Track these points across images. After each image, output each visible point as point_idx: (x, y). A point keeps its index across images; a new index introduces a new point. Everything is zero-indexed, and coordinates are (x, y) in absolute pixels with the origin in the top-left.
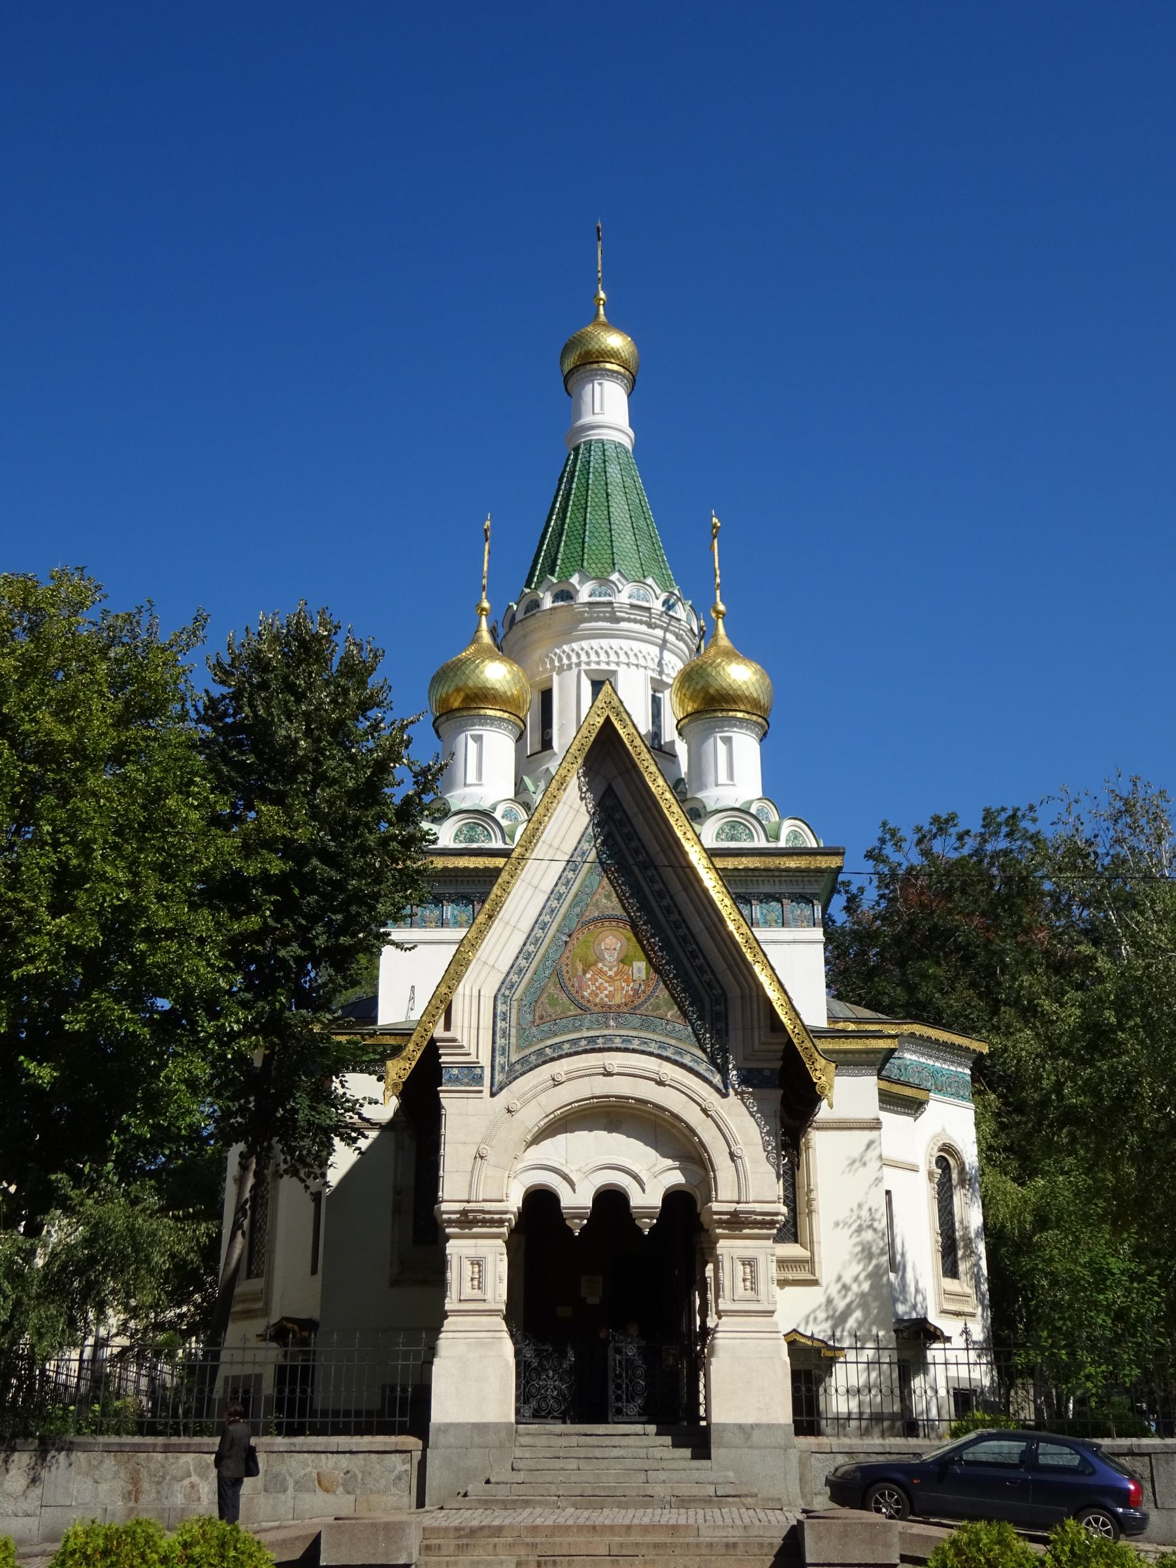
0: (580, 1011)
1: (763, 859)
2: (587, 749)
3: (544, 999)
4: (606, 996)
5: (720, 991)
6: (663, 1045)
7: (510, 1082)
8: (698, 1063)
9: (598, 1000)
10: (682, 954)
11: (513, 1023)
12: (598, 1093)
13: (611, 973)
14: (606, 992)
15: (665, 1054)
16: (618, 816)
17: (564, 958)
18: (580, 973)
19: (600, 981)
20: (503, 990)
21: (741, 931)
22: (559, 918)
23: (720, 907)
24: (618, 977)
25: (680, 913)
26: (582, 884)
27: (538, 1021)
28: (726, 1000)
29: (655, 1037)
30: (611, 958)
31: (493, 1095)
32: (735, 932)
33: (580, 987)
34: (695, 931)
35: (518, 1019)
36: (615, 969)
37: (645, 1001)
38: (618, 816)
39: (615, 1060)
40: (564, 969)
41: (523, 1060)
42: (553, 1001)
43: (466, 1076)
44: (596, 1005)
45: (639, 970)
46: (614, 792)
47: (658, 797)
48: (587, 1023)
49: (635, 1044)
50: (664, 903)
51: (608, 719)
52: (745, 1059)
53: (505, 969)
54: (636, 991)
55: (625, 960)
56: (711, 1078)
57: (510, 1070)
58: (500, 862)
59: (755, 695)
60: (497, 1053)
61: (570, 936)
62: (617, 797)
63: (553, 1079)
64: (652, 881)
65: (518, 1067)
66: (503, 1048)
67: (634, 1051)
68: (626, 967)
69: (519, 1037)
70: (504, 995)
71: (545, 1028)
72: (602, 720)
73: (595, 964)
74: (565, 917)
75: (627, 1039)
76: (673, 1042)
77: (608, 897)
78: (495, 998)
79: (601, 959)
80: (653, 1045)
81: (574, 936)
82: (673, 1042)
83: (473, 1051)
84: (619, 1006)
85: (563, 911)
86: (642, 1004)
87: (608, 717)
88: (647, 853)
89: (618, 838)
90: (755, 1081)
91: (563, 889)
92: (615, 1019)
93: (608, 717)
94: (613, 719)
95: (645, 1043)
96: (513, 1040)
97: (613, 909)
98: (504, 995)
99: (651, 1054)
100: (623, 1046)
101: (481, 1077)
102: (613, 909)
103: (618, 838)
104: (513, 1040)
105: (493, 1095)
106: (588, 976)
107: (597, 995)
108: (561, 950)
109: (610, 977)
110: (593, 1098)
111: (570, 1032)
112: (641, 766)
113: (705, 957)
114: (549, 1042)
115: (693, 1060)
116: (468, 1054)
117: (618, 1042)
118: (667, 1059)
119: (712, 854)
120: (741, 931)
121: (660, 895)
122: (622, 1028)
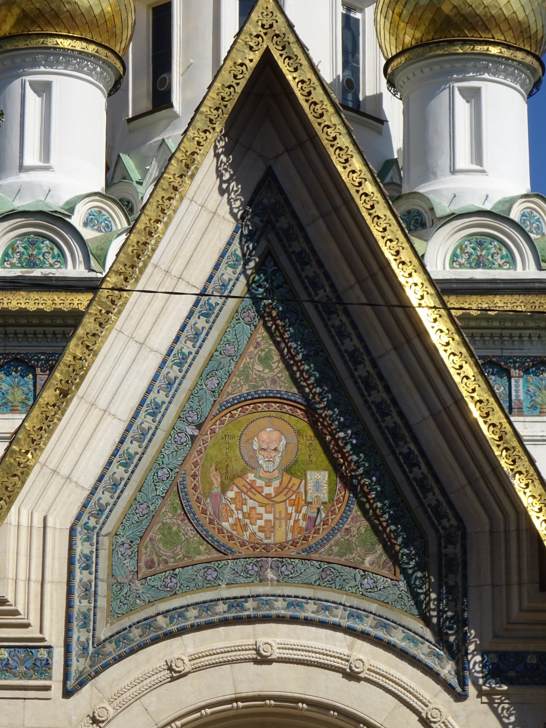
0: (215, 555)
1: (531, 298)
2: (230, 106)
3: (154, 533)
4: (261, 529)
5: (454, 522)
6: (356, 613)
7: (97, 673)
8: (416, 643)
9: (246, 536)
10: (390, 459)
11: (103, 573)
12: (245, 690)
14: (261, 523)
15: (359, 626)
16: (283, 222)
17: (189, 465)
18: (217, 490)
19: (251, 503)
20: (84, 519)
21: (493, 419)
22: (181, 396)
23: (457, 379)
25: (388, 390)
26: (220, 340)
27: (144, 570)
28: (464, 537)
29: (343, 598)
30: (269, 464)
31: (67, 694)
32: (481, 421)
33: (217, 515)
34: (413, 420)
35: (111, 566)
36: (276, 483)
37: (327, 539)
38: (283, 222)
39: (275, 637)
40: (190, 482)
41: (118, 637)
42: (170, 537)
43: (23, 662)
44: (243, 544)
45: (317, 485)
46: (276, 180)
47: (353, 191)
48: (227, 574)
50: (361, 371)
51: (267, 53)
52: (495, 636)
53: (89, 482)
54: (312, 521)
55: (293, 469)
56: (437, 668)
57: (97, 653)
58: (80, 301)
59: (521, 16)
60: (75, 624)
61: (199, 427)
62: (281, 191)
63: (170, 669)
64: (341, 333)
65: (109, 647)
66: (86, 617)
67: (307, 622)
68: (295, 481)
69: (112, 597)
70: (86, 526)
72: (256, 56)
73: (242, 474)
74: (192, 395)
75: (296, 602)
76: (374, 607)
77: (265, 361)
78: (72, 531)
79: (254, 467)
80: (340, 611)
81: (207, 427)
82: (374, 607)
83: (34, 619)
84: (282, 546)
85: (187, 384)
86: (321, 543)
87: (267, 51)
88: (332, 286)
89: (283, 260)
90: (512, 674)
91: (187, 347)
92: (275, 568)
94: (276, 54)
95: (327, 608)
96: (102, 602)
97: (274, 381)
98: (86, 526)
99: (336, 627)
100: (289, 613)
101: (48, 664)
102: (274, 381)
103: (283, 260)
104: (102, 602)
106: (231, 494)
107: (245, 527)
110: (236, 700)
111: (199, 589)
112: (323, 137)
113: (428, 464)
114: (163, 606)
116: (27, 626)
117: (280, 607)
118: (364, 636)
119: (444, 289)
120: (493, 419)
121: (353, 358)
122: (287, 584)
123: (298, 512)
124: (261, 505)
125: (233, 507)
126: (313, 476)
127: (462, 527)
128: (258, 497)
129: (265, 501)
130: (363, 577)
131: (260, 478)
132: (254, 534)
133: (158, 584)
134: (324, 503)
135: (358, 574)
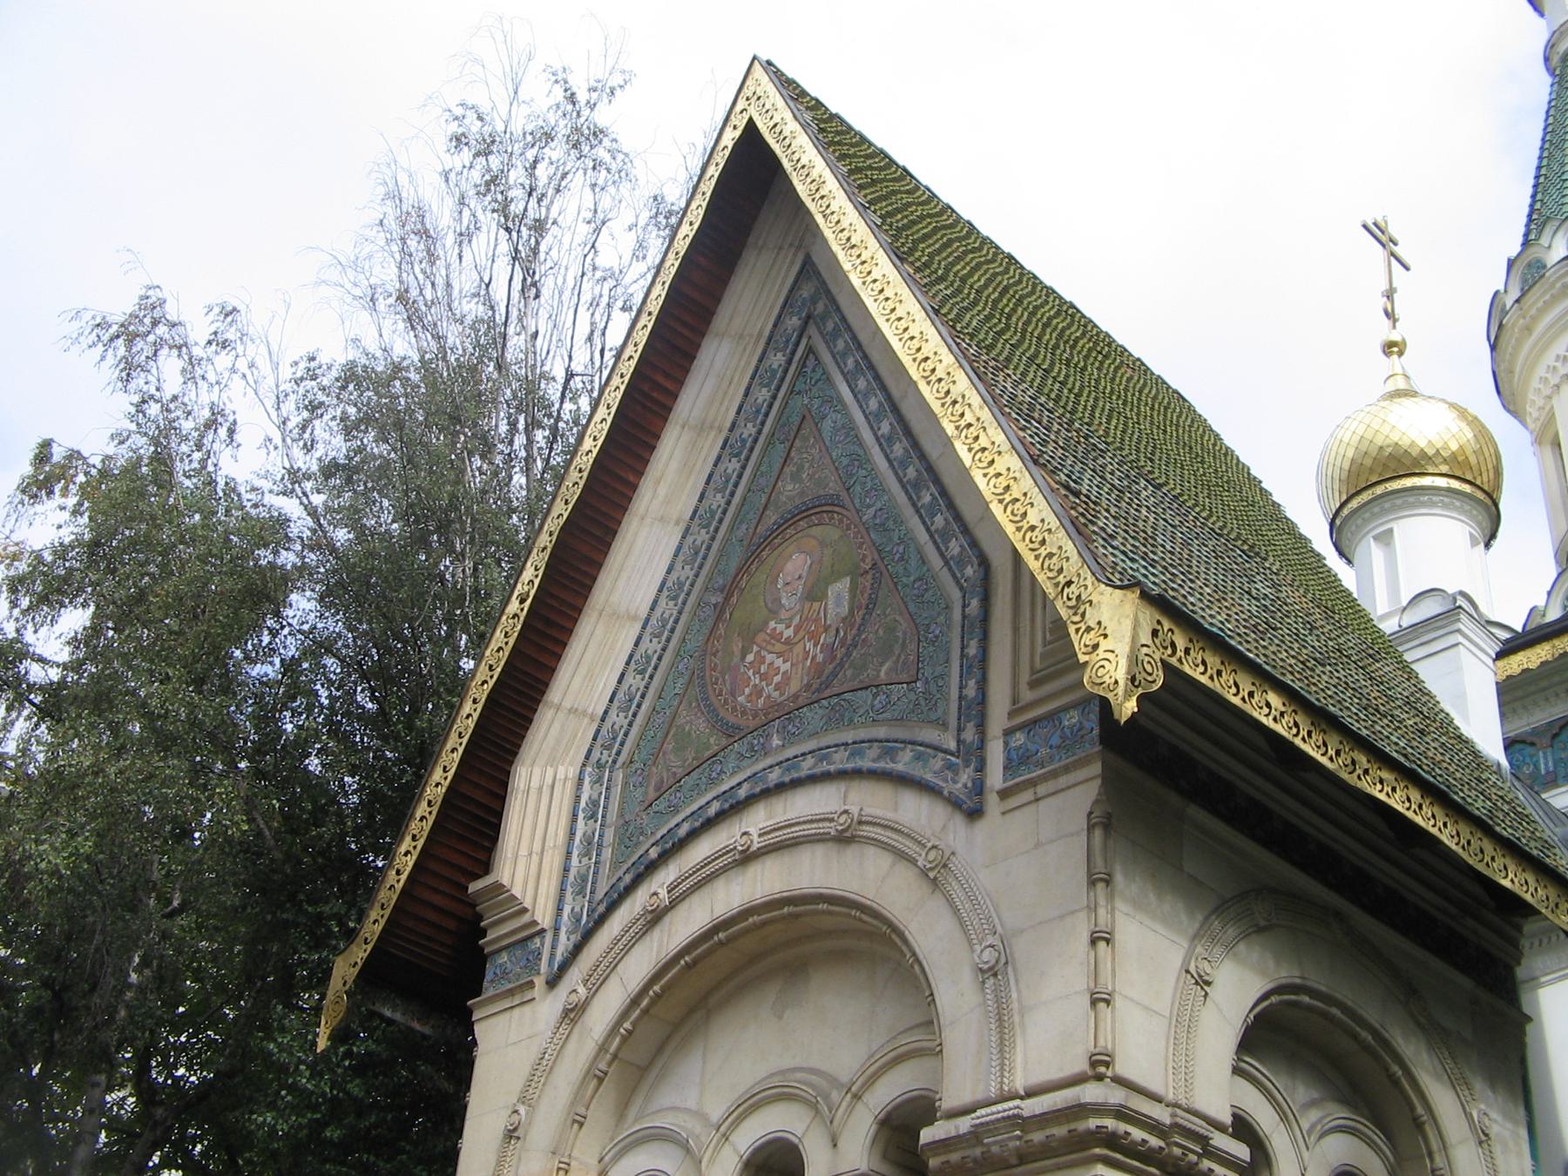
13: (789, 633)
14: (777, 679)
16: (820, 307)
18: (736, 660)
19: (769, 658)
20: (596, 755)
24: (802, 633)
36: (796, 620)
45: (839, 597)
46: (813, 264)
49: (807, 767)
54: (830, 650)
55: (814, 593)
68: (816, 605)
71: (661, 805)
75: (790, 763)
76: (881, 732)
77: (796, 477)
84: (796, 696)
86: (834, 674)
87: (751, 119)
93: (751, 119)
94: (756, 118)
96: (607, 853)
97: (802, 493)
104: (607, 853)
105: (552, 983)
106: (750, 658)
108: (710, 623)
109: (788, 642)
115: (919, 757)
117: (774, 777)
123: (815, 646)
124: (779, 655)
125: (750, 673)
126: (832, 591)
127: (984, 563)
128: (779, 647)
129: (785, 648)
130: (875, 696)
131: (780, 621)
132: (769, 696)
133: (661, 808)
134: (844, 620)
135: (866, 695)
